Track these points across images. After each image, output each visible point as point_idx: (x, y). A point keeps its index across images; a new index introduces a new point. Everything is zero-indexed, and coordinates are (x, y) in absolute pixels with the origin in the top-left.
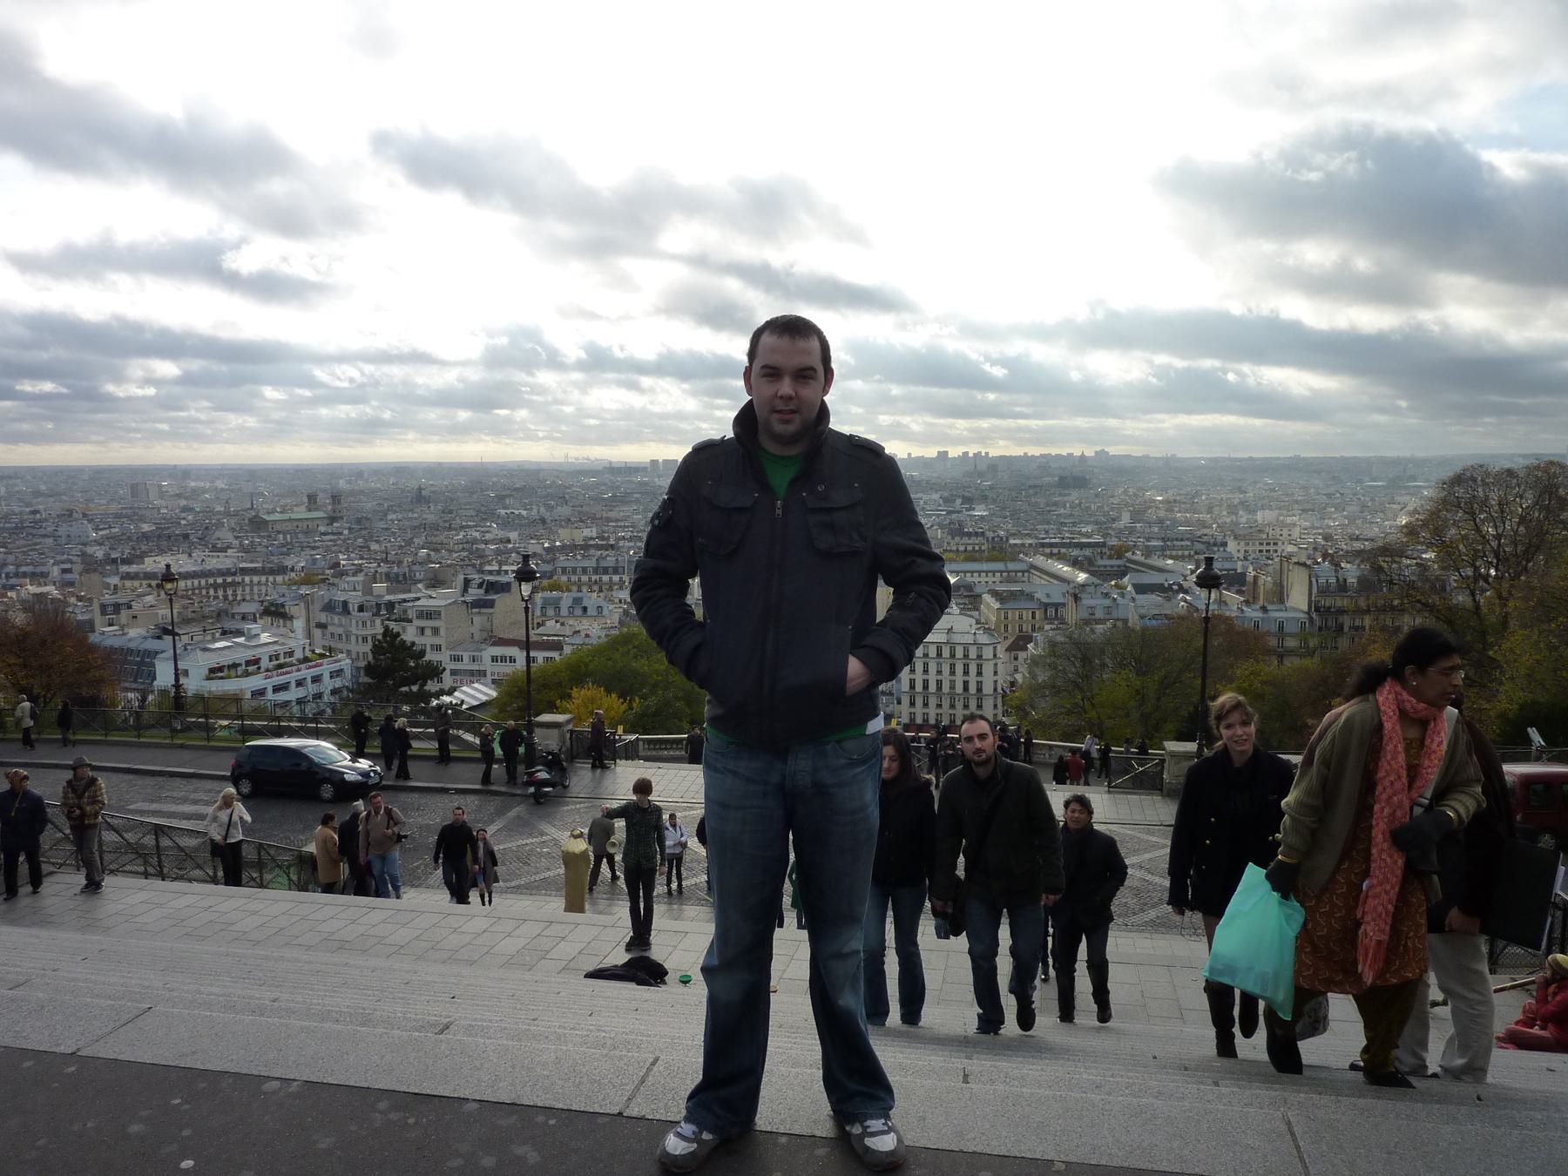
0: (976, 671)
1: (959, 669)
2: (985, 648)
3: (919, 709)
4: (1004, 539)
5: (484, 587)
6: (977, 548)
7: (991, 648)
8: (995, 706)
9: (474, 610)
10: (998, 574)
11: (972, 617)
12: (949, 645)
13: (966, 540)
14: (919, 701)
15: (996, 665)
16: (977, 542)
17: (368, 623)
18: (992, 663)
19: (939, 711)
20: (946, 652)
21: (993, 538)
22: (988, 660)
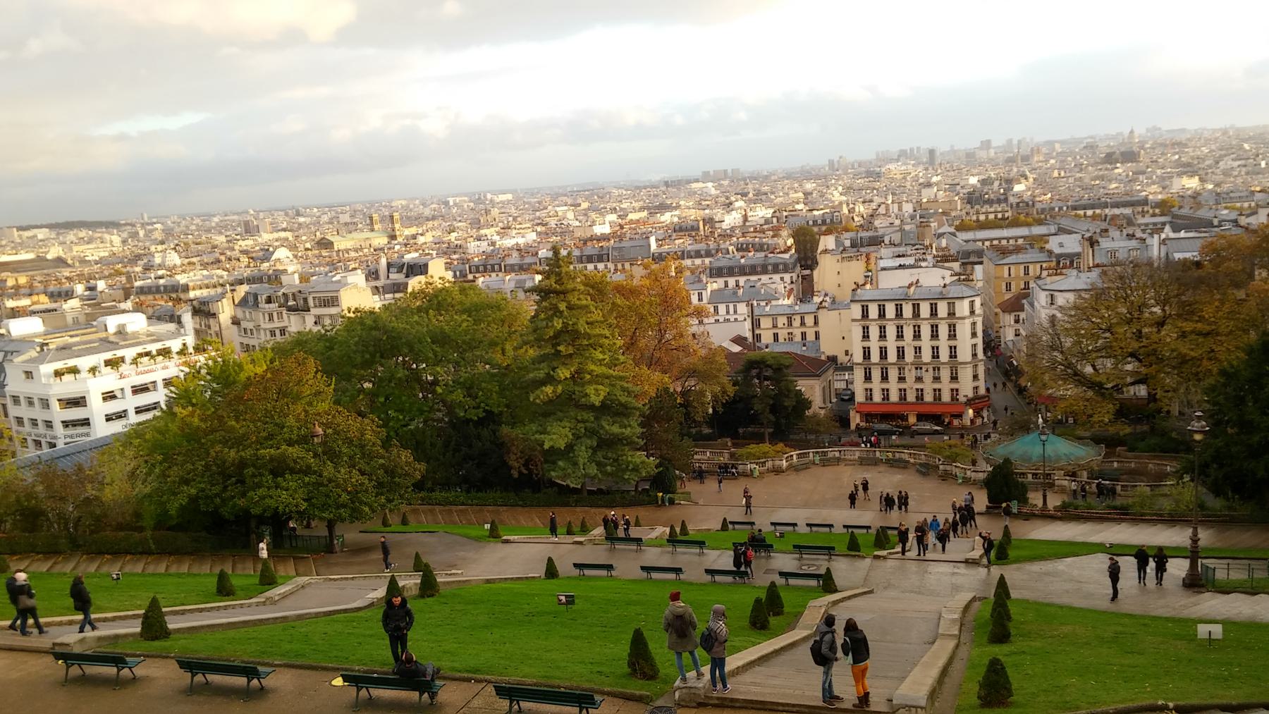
1: (926, 331)
2: (957, 303)
3: (876, 385)
4: (1031, 203)
5: (405, 271)
6: (1000, 216)
7: (966, 303)
8: (975, 377)
9: (387, 296)
12: (910, 303)
13: (987, 208)
14: (876, 374)
15: (974, 324)
16: (999, 209)
17: (275, 315)
18: (968, 322)
19: (903, 386)
20: (908, 311)
21: (1018, 204)
22: (963, 318)
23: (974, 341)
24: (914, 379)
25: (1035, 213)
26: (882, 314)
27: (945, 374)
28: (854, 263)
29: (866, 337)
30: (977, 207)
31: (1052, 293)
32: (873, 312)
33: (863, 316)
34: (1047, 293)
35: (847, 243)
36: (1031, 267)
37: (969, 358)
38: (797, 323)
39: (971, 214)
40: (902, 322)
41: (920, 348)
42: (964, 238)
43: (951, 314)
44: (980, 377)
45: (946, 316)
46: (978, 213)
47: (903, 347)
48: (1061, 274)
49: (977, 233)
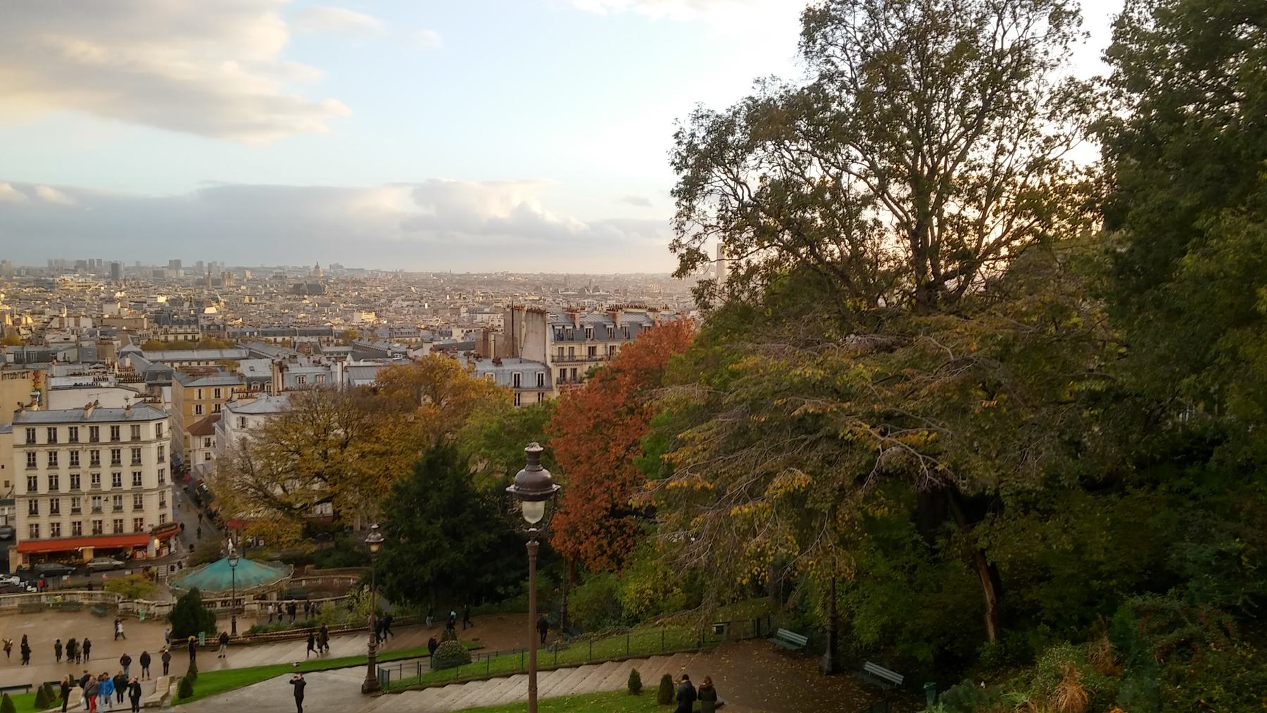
0: (130, 458)
1: (105, 457)
2: (143, 426)
3: (44, 519)
4: (222, 326)
6: (190, 337)
7: (152, 426)
8: (162, 504)
12: (88, 426)
13: (175, 328)
14: (44, 507)
15: (161, 448)
16: (189, 331)
18: (154, 446)
19: (77, 518)
20: (84, 434)
21: (209, 327)
22: (150, 442)
23: (161, 466)
24: (91, 510)
25: (226, 336)
26: (52, 439)
27: (128, 503)
28: (18, 382)
29: (32, 464)
30: (165, 327)
31: (243, 416)
32: (42, 435)
34: (238, 416)
35: (10, 358)
36: (222, 390)
37: (155, 484)
40: (77, 447)
41: (98, 476)
42: (151, 358)
43: (136, 438)
44: (167, 504)
45: (129, 440)
46: (166, 333)
47: (78, 476)
48: (252, 397)
49: (165, 354)
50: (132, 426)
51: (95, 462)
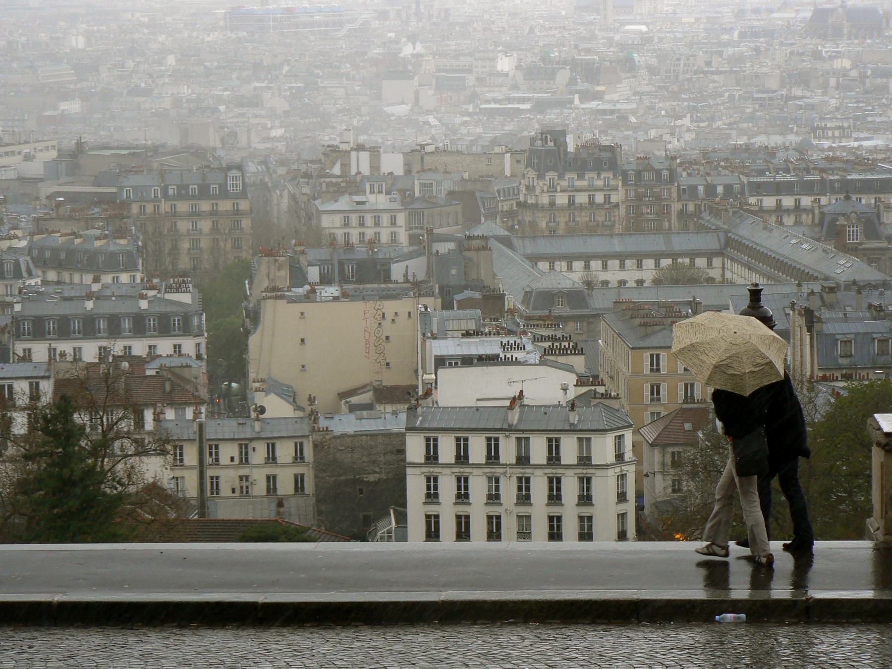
1: (539, 488)
4: (665, 173)
6: (599, 198)
7: (609, 440)
10: (649, 263)
11: (569, 369)
12: (513, 437)
15: (622, 477)
16: (599, 183)
18: (612, 473)
20: (508, 451)
22: (605, 467)
23: (622, 508)
33: (428, 458)
38: (259, 454)
39: (538, 191)
43: (585, 461)
46: (552, 189)
47: (499, 517)
50: (580, 439)
51: (524, 498)
